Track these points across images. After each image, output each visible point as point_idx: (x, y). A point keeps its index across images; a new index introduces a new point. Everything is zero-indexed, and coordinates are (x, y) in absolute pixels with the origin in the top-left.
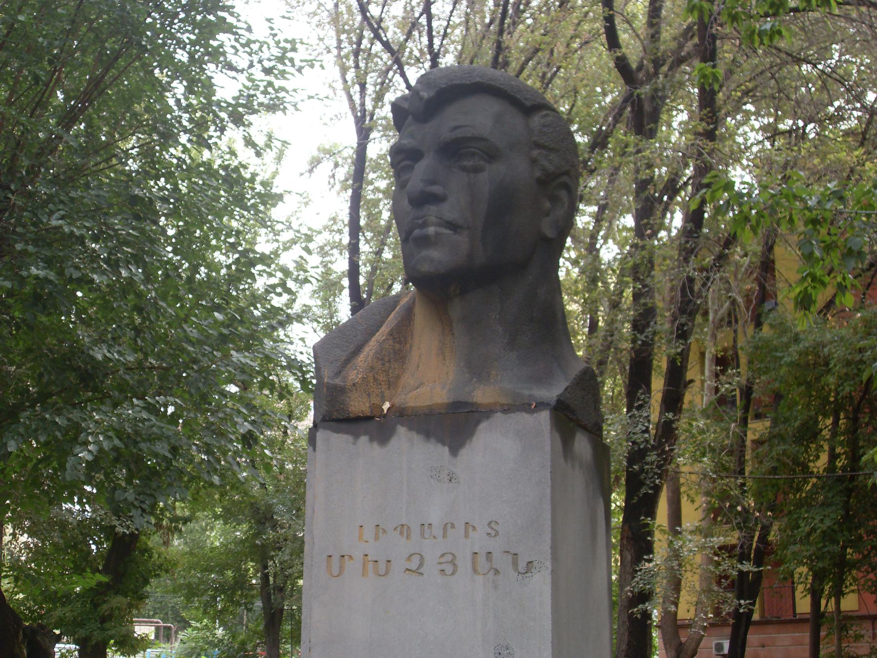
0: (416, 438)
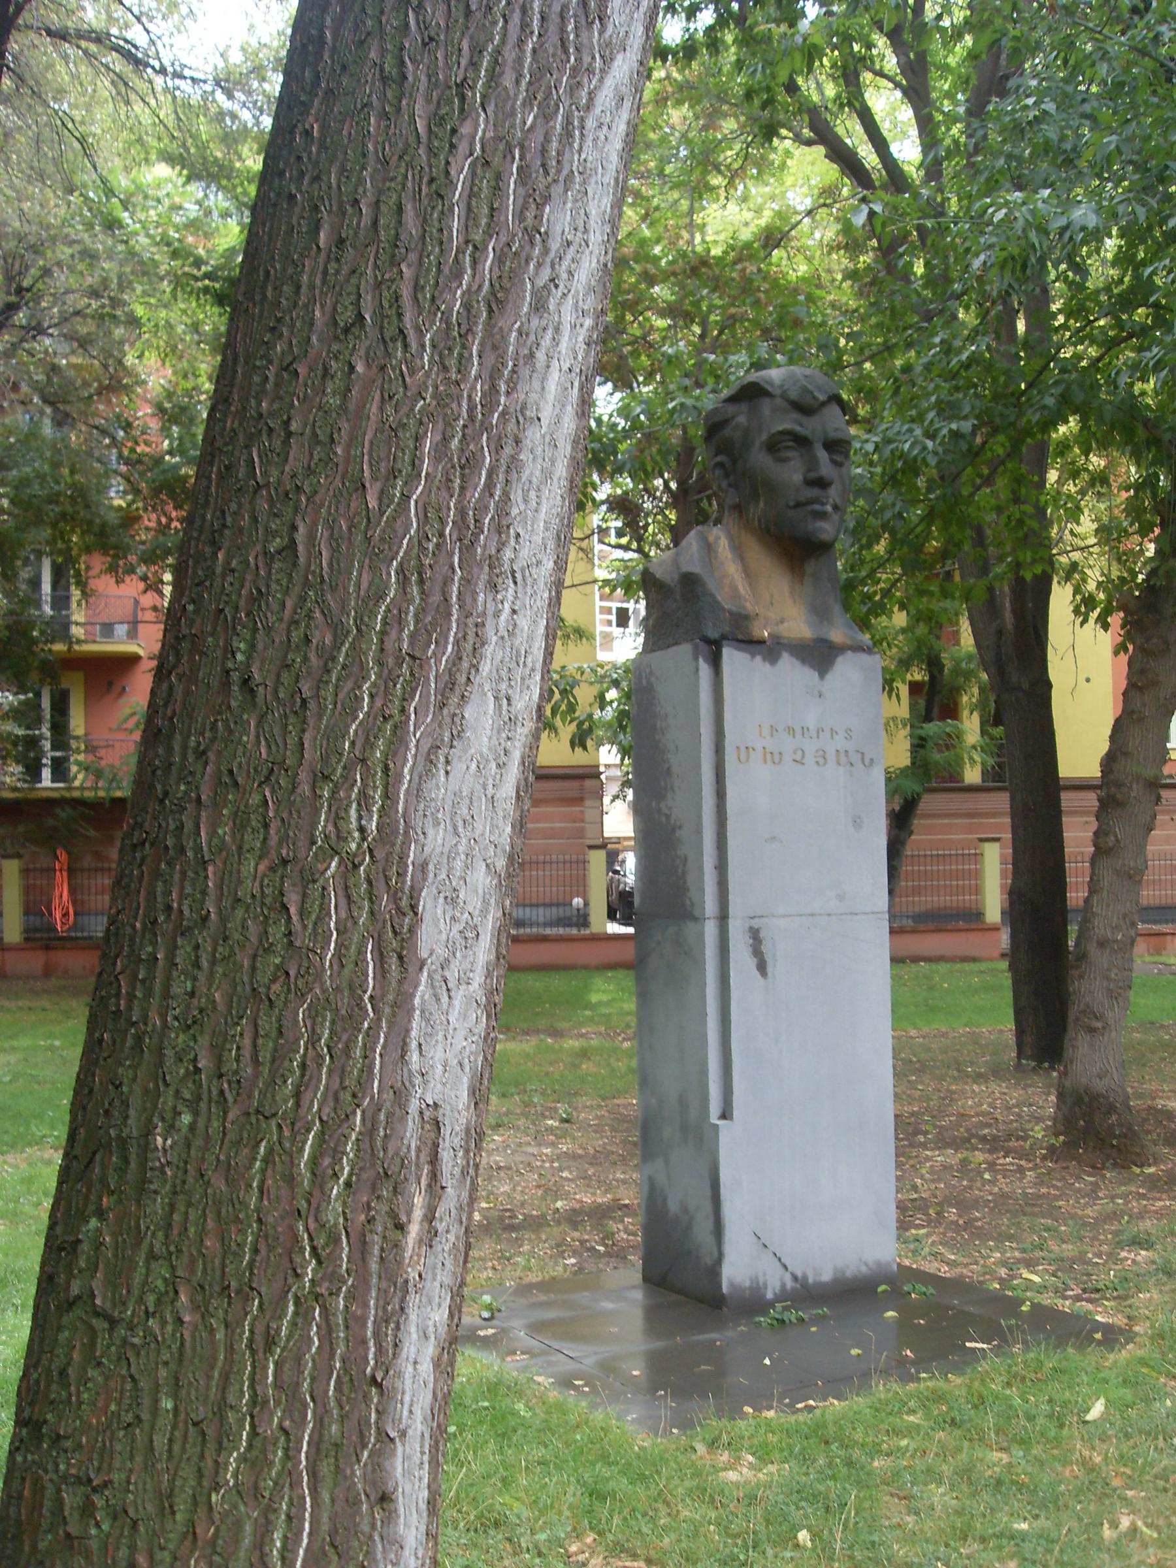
0: (797, 663)
